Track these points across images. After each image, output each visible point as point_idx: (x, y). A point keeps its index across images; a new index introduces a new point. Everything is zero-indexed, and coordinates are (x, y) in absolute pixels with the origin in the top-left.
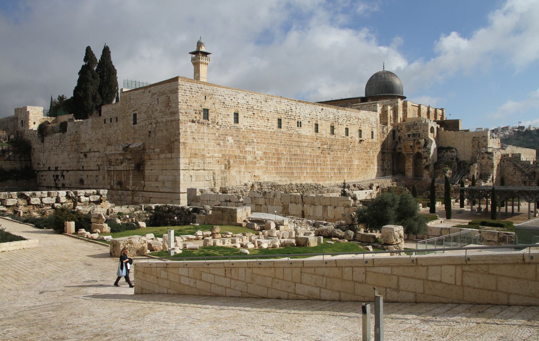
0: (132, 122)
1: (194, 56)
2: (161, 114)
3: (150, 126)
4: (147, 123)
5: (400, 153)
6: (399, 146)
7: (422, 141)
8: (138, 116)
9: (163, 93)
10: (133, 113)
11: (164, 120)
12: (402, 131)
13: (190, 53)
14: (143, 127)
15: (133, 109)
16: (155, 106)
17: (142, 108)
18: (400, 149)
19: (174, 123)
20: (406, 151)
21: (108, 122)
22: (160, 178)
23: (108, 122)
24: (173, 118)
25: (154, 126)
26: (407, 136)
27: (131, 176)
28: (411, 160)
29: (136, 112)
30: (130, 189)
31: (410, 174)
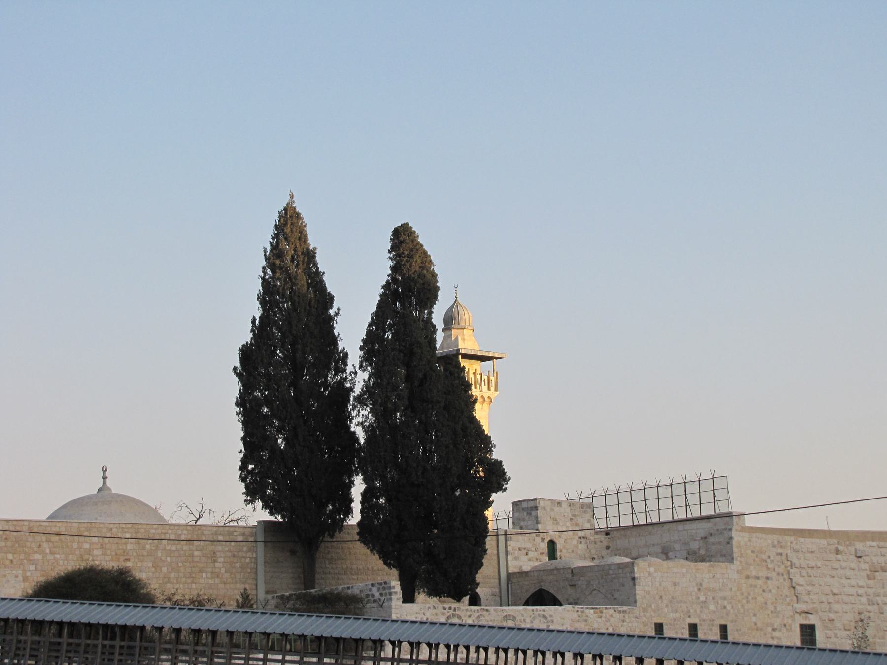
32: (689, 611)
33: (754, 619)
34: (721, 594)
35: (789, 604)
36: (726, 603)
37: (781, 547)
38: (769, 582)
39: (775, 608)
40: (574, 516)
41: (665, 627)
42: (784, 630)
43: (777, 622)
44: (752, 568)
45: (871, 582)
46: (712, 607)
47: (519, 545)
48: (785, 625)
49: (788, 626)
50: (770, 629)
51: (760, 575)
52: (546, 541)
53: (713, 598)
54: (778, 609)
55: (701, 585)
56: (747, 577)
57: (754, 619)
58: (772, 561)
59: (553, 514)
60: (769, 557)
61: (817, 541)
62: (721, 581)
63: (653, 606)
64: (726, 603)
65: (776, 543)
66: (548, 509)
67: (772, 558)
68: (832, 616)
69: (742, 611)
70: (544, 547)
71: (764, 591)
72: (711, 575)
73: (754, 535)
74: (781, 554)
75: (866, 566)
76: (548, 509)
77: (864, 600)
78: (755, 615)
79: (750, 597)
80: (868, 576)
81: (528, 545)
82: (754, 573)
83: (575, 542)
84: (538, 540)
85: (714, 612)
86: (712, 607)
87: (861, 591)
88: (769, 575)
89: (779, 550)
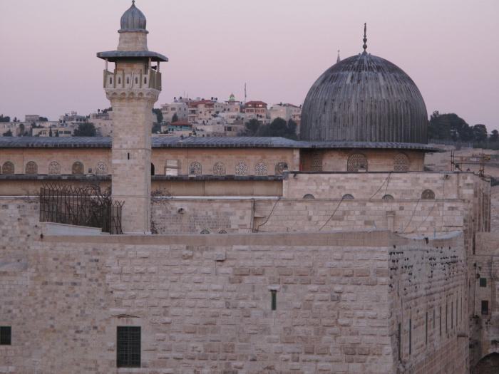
0: (113, 356)
1: (112, 66)
2: (289, 348)
8: (146, 340)
9: (305, 277)
10: (123, 323)
13: (99, 55)
15: (123, 311)
17: (173, 311)
29: (136, 324)
33: (51, 322)
35: (104, 308)
36: (11, 307)
37: (98, 254)
38: (76, 288)
39: (83, 312)
40: (24, 216)
42: (95, 331)
43: (83, 325)
44: (52, 275)
45: (234, 287)
48: (95, 328)
49: (99, 328)
50: (72, 331)
51: (64, 281)
54: (86, 312)
56: (46, 283)
57: (51, 322)
58: (84, 267)
60: (79, 264)
61: (155, 246)
62: (7, 287)
64: (11, 307)
65: (90, 250)
67: (83, 265)
68: (167, 319)
71: (67, 296)
73: (60, 244)
74: (97, 261)
75: (229, 270)
77: (221, 303)
78: (51, 318)
79: (47, 302)
80: (230, 279)
82: (55, 279)
83: (22, 240)
87: (218, 295)
88: (76, 281)
89: (94, 257)
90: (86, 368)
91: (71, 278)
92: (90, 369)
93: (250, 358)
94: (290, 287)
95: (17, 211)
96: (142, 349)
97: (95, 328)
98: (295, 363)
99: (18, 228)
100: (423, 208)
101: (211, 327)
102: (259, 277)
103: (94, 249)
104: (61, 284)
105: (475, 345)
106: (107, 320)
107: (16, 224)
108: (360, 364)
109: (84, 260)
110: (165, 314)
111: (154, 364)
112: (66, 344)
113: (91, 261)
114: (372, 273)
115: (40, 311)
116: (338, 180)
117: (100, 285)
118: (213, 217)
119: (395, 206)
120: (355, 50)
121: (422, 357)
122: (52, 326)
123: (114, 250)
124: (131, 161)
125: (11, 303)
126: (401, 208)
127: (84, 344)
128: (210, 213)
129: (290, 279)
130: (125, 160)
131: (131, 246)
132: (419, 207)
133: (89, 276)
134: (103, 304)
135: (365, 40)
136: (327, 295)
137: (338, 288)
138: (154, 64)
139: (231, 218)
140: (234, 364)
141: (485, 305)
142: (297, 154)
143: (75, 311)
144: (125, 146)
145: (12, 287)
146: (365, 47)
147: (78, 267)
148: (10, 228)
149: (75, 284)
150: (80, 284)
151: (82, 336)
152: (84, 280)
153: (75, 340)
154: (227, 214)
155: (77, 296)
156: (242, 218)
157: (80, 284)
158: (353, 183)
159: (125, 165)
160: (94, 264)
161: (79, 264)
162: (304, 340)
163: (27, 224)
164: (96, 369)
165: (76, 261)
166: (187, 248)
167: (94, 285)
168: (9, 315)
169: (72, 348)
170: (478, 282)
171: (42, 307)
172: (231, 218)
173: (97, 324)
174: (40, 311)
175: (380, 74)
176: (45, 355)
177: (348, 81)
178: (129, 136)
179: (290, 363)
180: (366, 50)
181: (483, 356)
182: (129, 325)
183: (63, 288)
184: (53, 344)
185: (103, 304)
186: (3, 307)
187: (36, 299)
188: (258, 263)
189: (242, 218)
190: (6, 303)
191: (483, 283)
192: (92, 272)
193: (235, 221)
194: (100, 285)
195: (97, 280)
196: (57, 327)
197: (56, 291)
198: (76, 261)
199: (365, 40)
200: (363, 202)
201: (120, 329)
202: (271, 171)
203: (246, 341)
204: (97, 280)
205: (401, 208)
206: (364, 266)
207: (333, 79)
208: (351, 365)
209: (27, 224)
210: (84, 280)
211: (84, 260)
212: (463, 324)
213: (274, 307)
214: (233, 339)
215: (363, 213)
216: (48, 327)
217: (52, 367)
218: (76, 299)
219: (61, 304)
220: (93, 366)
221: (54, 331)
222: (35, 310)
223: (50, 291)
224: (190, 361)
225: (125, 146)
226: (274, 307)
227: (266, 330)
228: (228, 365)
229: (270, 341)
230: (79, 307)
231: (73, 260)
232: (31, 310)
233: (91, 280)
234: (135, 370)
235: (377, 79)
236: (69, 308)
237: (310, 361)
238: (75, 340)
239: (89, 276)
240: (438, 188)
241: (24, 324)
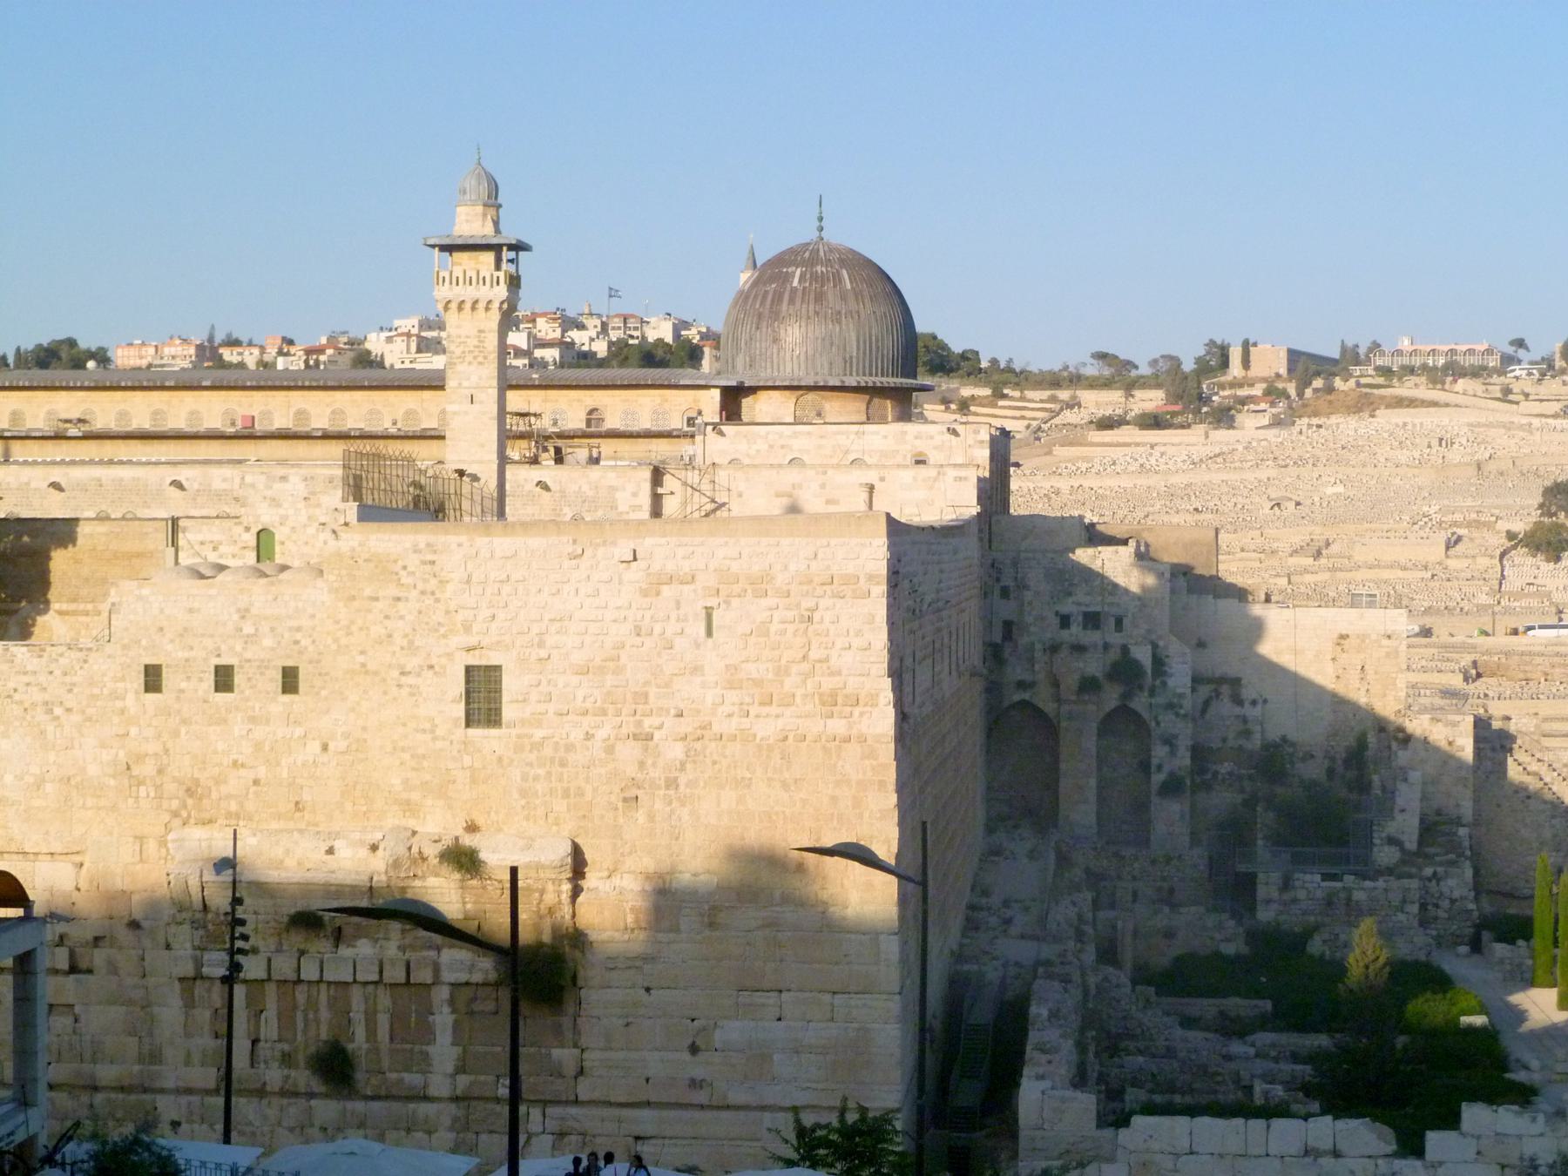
2: (733, 696)
3: (628, 753)
4: (601, 734)
5: (1024, 704)
6: (1016, 671)
7: (1143, 655)
8: (510, 685)
9: (760, 585)
11: (767, 728)
12: (1028, 595)
14: (570, 748)
15: (473, 641)
16: (679, 643)
18: (1022, 685)
19: (854, 749)
20: (1058, 699)
21: (189, 685)
22: (732, 1031)
23: (189, 685)
24: (837, 726)
25: (676, 751)
26: (1057, 621)
27: (443, 1019)
28: (1090, 743)
29: (493, 661)
30: (439, 1085)
31: (1080, 809)
32: (219, 648)
33: (361, 659)
34: (294, 623)
35: (445, 636)
36: (298, 636)
38: (401, 605)
39: (411, 642)
41: (164, 670)
43: (412, 663)
46: (268, 642)
47: (200, 537)
48: (431, 667)
50: (395, 673)
51: (381, 594)
52: (254, 530)
53: (272, 629)
54: (417, 643)
55: (247, 610)
56: (353, 598)
57: (361, 659)
59: (269, 493)
60: (405, 568)
63: (144, 642)
64: (298, 636)
65: (422, 546)
66: (261, 486)
68: (543, 653)
69: (334, 647)
70: (251, 539)
71: (387, 617)
72: (270, 597)
74: (433, 563)
76: (261, 486)
78: (362, 653)
79: (354, 628)
81: (217, 537)
82: (368, 592)
83: (311, 531)
84: (240, 529)
85: (273, 649)
86: (268, 642)
89: (430, 557)
90: (417, 730)
91: (392, 591)
92: (424, 731)
93: (673, 712)
94: (735, 602)
95: (301, 486)
96: (505, 699)
97: (431, 667)
98: (744, 720)
99: (303, 512)
100: (915, 479)
101: (611, 664)
102: (686, 588)
103: (428, 545)
104: (377, 599)
105: (993, 689)
106: (449, 655)
107: (301, 505)
108: (844, 721)
109: (413, 561)
110: (541, 645)
111: (523, 722)
112: (385, 693)
113: (424, 563)
114: (862, 581)
115: (344, 641)
116: (781, 435)
117: (437, 600)
118: (590, 493)
119: (871, 476)
120: (807, 234)
121: (928, 708)
122: (363, 665)
123: (460, 545)
124: (476, 407)
125: (299, 629)
126: (882, 479)
127: (414, 692)
128: (585, 488)
129: (737, 588)
130: (467, 406)
131: (486, 540)
132: (907, 475)
133: (420, 586)
134: (442, 630)
135: (821, 219)
136: (790, 615)
137: (810, 603)
138: (512, 255)
139: (618, 495)
140: (647, 722)
141: (1008, 625)
142: (716, 393)
143: (399, 641)
144: (465, 384)
145: (300, 605)
146: (821, 229)
147: (403, 573)
148: (291, 512)
149: (399, 599)
150: (407, 599)
151: (410, 680)
152: (414, 594)
153: (399, 686)
154: (613, 489)
155: (402, 618)
156: (635, 495)
157: (407, 599)
158: (804, 440)
159: (466, 413)
160: (428, 568)
161: (405, 568)
162: (758, 683)
163: (319, 505)
164: (433, 732)
165: (400, 563)
166: (575, 541)
167: (429, 601)
168: (296, 647)
169: (395, 699)
170: (997, 592)
171: (349, 634)
172: (618, 495)
173: (434, 661)
174: (344, 641)
175: (844, 272)
176: (353, 710)
177: (795, 283)
178: (472, 368)
179: (735, 720)
180: (824, 234)
181: (1006, 704)
182: (484, 662)
183: (379, 605)
184: (365, 692)
185: (442, 630)
186: (287, 635)
187: (337, 622)
188: (686, 567)
189: (635, 495)
190: (290, 629)
191: (1005, 593)
192: (425, 581)
193: (624, 500)
194: (437, 600)
195: (433, 593)
196: (371, 666)
197: (369, 611)
198: (400, 563)
199: (821, 219)
200: (823, 469)
201: (469, 670)
202: (677, 423)
203: (667, 685)
204: (433, 593)
205: (882, 479)
206: (850, 568)
207: (771, 280)
208: (829, 722)
209: (319, 505)
210: (414, 594)
211: (413, 561)
212: (973, 654)
213: (709, 633)
214: (647, 683)
215: (823, 486)
216: (357, 667)
217: (364, 729)
218: (401, 623)
219: (378, 630)
220: (428, 726)
221: (367, 673)
222: (336, 640)
223: (358, 611)
224: (580, 718)
225: (465, 384)
226: (709, 633)
227: (697, 670)
228: (639, 724)
229: (703, 685)
230: (406, 636)
231: (395, 561)
232: (330, 641)
233: (423, 593)
234: (493, 732)
235: (838, 279)
236: (390, 636)
237: (767, 715)
238: (399, 686)
239: (420, 586)
240: (935, 448)
241: (318, 662)
